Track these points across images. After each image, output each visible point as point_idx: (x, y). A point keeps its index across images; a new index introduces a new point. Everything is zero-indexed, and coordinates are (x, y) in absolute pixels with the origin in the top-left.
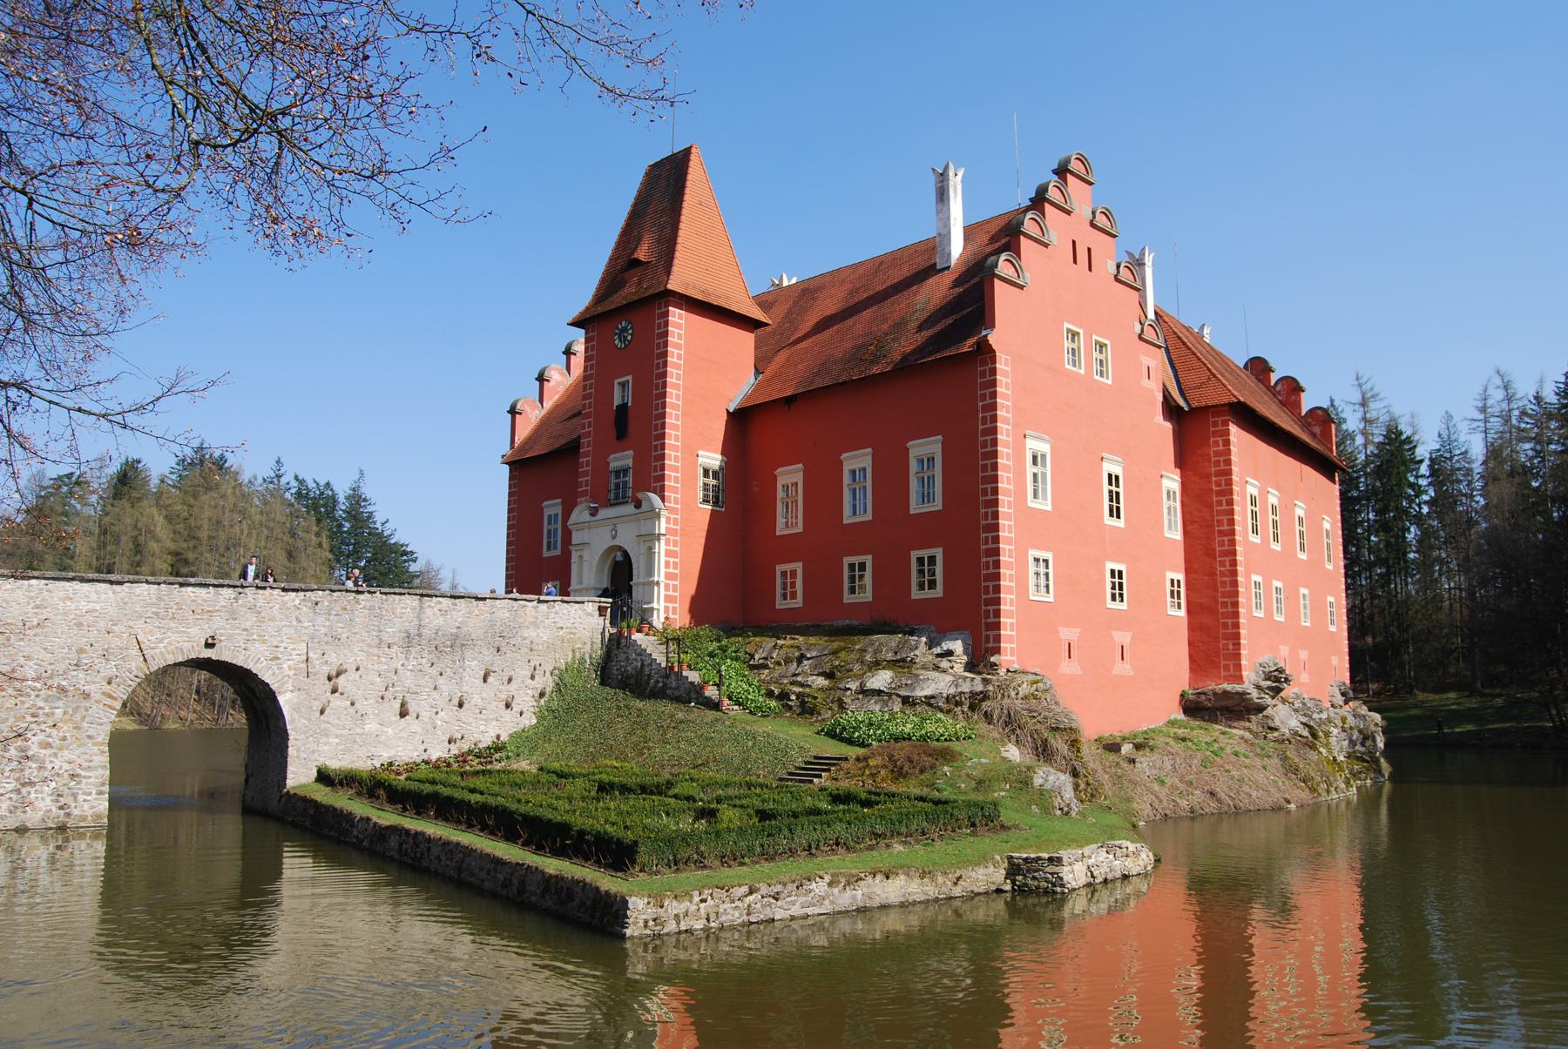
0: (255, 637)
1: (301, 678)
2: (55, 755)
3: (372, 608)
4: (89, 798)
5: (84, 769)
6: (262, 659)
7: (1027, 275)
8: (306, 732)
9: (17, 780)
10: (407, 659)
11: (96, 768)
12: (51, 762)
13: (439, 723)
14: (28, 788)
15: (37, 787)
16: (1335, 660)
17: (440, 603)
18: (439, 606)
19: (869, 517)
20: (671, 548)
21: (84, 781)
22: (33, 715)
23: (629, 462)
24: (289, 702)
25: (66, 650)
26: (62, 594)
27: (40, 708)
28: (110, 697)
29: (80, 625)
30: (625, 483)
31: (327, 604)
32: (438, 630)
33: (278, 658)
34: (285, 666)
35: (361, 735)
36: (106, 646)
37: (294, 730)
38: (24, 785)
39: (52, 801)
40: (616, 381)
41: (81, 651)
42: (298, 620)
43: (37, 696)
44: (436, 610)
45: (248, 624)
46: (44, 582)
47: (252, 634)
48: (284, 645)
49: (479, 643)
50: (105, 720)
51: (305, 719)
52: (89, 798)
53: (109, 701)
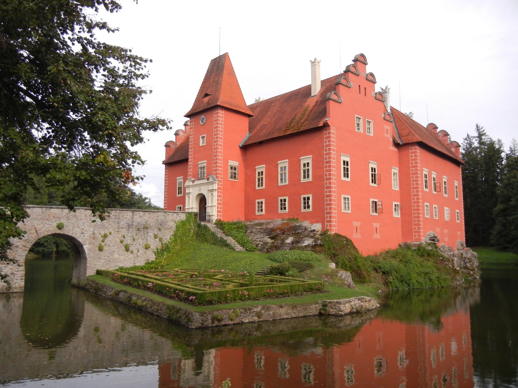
2: (6, 267)
3: (116, 216)
4: (18, 281)
5: (16, 271)
7: (342, 98)
8: (93, 258)
11: (20, 271)
12: (5, 269)
13: (139, 255)
16: (459, 233)
17: (139, 214)
19: (287, 183)
20: (219, 194)
21: (16, 275)
23: (205, 165)
24: (87, 248)
28: (25, 247)
30: (204, 172)
33: (83, 233)
34: (86, 235)
35: (112, 259)
37: (89, 257)
40: (201, 136)
44: (138, 216)
48: (86, 228)
50: (24, 254)
52: (18, 281)
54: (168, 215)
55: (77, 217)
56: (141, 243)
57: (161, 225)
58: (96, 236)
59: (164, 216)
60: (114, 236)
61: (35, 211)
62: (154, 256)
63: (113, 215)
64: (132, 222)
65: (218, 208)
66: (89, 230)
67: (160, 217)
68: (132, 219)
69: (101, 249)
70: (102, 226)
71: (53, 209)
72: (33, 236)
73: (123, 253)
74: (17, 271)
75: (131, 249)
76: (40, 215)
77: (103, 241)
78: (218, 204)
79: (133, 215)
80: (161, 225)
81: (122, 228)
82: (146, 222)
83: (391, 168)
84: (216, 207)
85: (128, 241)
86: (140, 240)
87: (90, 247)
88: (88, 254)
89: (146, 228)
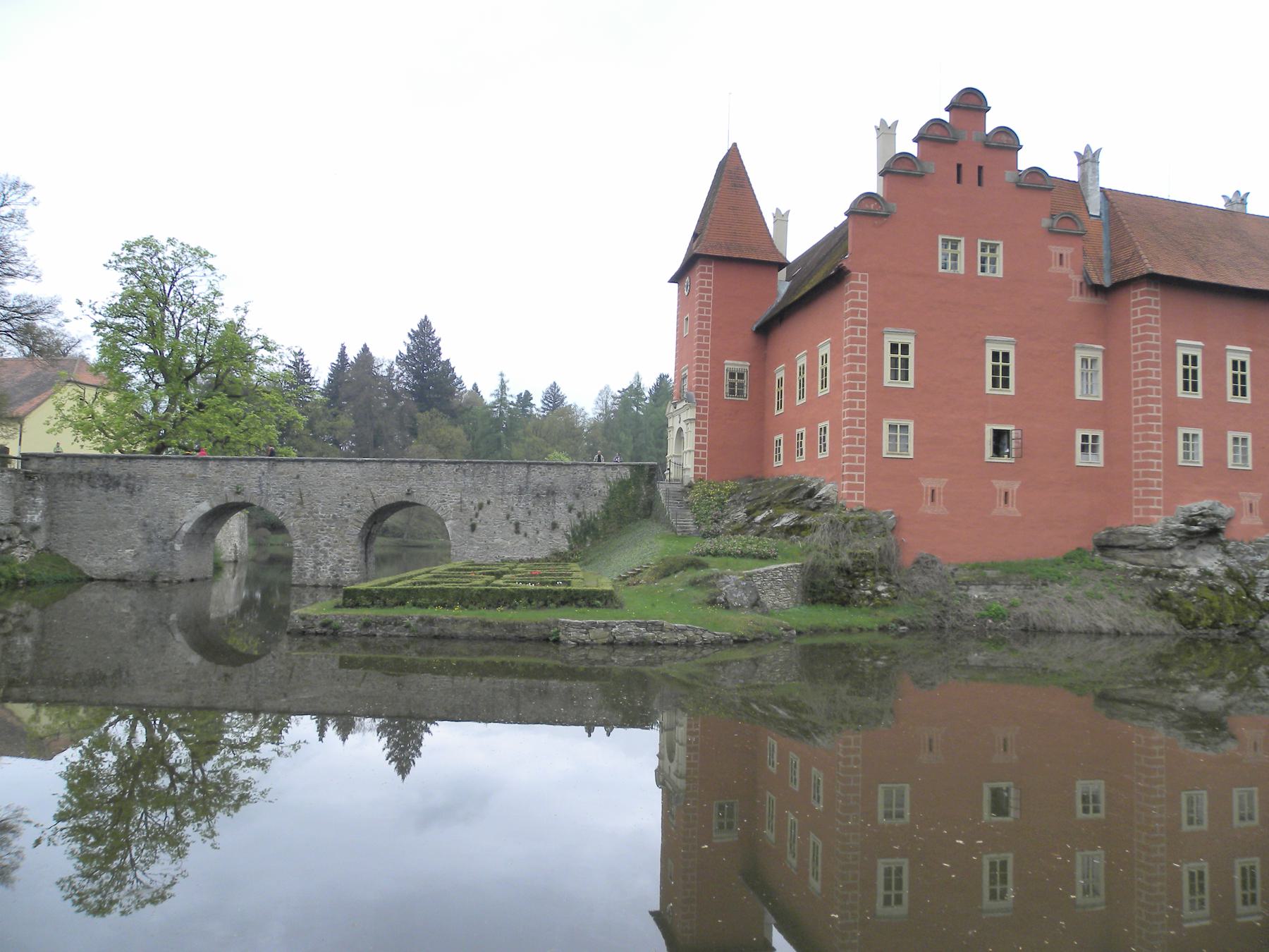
3: (498, 472)
9: (314, 561)
22: (322, 530)
24: (451, 525)
26: (334, 469)
29: (343, 484)
38: (318, 564)
41: (343, 498)
54: (596, 469)
57: (581, 489)
58: (465, 506)
59: (586, 472)
61: (371, 466)
62: (567, 543)
65: (696, 454)
68: (527, 477)
69: (473, 528)
71: (397, 465)
72: (369, 505)
74: (347, 558)
75: (523, 529)
76: (378, 473)
77: (477, 515)
78: (697, 447)
80: (581, 489)
81: (509, 493)
83: (1074, 349)
84: (693, 453)
85: (520, 515)
89: (551, 492)
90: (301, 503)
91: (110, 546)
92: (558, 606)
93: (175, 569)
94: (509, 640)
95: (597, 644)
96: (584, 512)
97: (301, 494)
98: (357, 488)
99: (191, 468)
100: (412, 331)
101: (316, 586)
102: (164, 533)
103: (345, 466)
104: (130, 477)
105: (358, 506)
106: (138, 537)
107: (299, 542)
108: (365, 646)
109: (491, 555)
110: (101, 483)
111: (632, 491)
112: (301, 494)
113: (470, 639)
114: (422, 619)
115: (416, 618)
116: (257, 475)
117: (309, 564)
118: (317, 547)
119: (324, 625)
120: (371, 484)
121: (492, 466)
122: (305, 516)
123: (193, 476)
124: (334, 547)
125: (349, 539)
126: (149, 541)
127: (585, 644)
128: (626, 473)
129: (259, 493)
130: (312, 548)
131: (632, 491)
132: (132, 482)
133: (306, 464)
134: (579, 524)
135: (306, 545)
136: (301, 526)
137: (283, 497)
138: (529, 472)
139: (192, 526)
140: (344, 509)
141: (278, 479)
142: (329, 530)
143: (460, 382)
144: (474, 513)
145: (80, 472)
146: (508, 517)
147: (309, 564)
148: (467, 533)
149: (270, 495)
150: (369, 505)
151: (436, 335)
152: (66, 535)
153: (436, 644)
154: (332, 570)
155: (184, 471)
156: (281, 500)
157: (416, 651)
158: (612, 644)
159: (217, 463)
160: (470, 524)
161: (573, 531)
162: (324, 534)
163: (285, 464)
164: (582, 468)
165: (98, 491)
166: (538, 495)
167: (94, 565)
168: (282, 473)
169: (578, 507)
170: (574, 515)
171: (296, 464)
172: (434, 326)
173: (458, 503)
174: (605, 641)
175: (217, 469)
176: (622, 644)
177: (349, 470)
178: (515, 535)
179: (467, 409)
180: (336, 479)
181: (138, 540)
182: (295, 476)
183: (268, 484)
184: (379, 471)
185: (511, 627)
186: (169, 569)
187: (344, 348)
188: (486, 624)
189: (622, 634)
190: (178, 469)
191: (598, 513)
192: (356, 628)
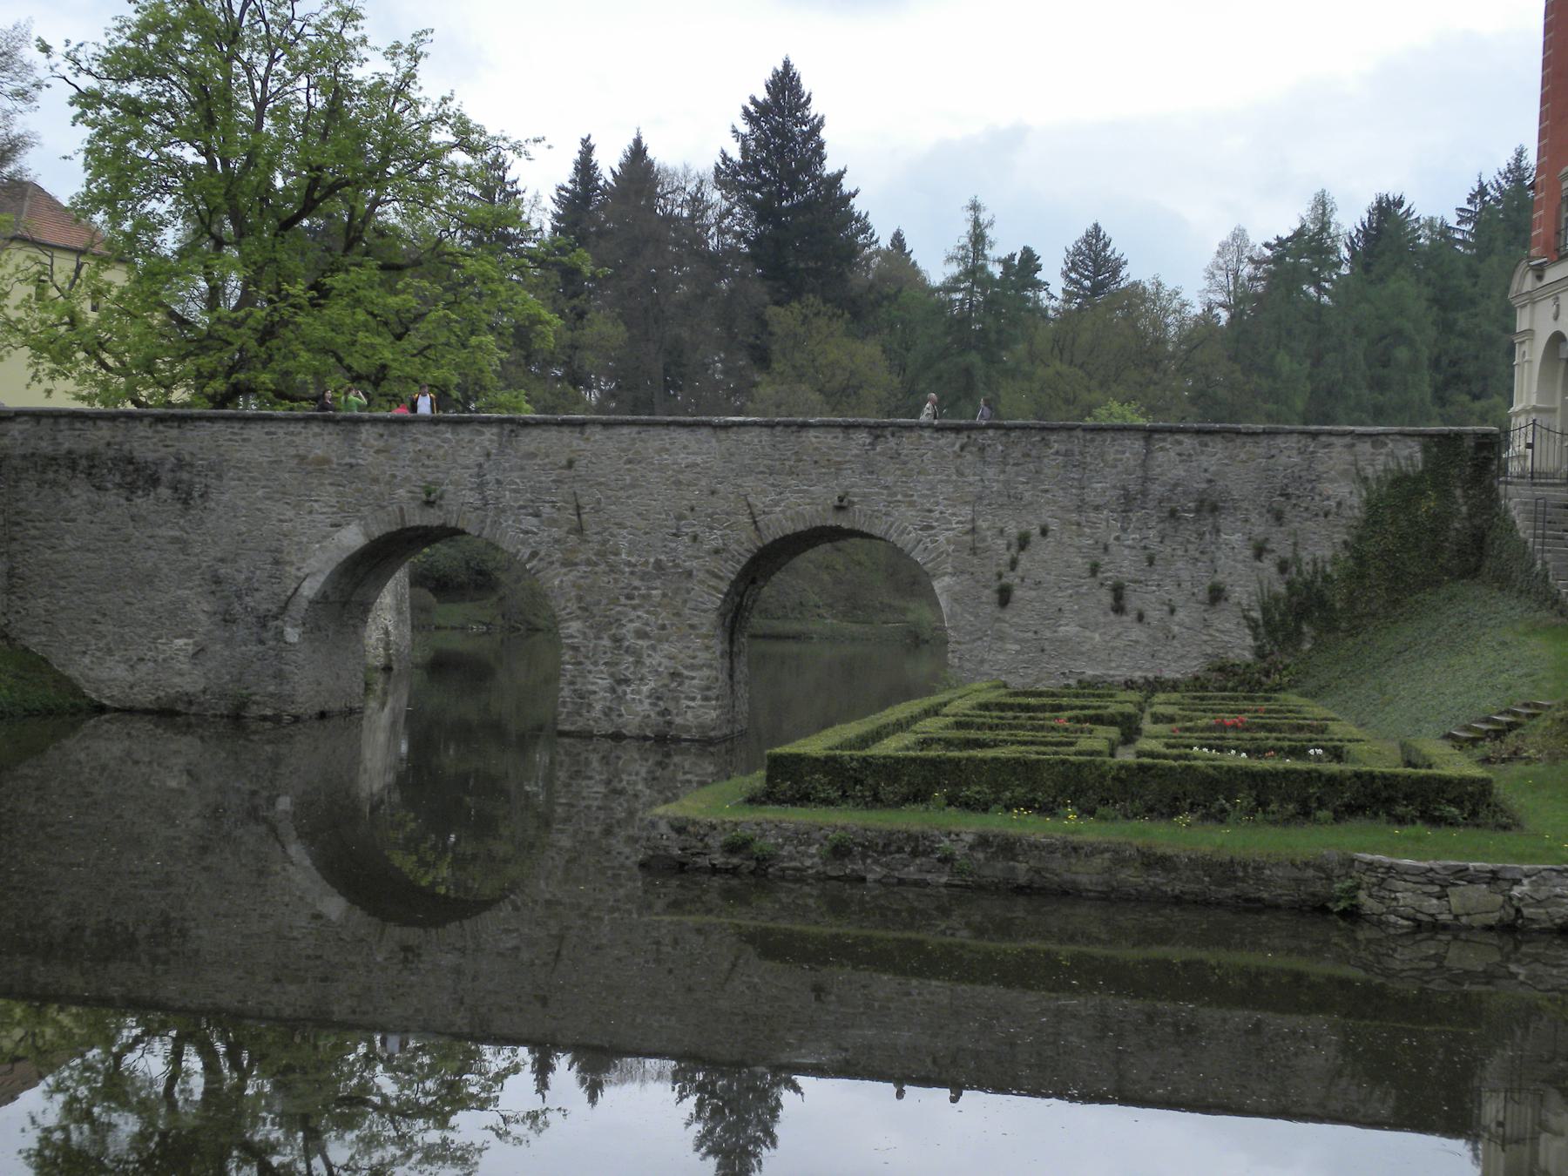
0: (899, 497)
1: (965, 555)
2: (653, 648)
3: (1068, 453)
4: (692, 704)
5: (686, 667)
6: (910, 528)
8: (971, 633)
9: (612, 675)
10: (1124, 530)
11: (701, 667)
12: (649, 656)
13: (1176, 629)
14: (624, 687)
15: (633, 687)
17: (1180, 443)
18: (1178, 448)
22: (629, 597)
24: (948, 589)
25: (664, 516)
26: (657, 444)
27: (636, 588)
29: (678, 483)
31: (1000, 448)
32: (1176, 485)
33: (932, 528)
34: (941, 538)
36: (710, 511)
37: (954, 628)
38: (619, 682)
39: (651, 704)
41: (680, 517)
42: (960, 473)
43: (632, 573)
44: (1172, 454)
45: (890, 479)
46: (635, 429)
47: (895, 494)
48: (941, 508)
49: (1245, 505)
50: (709, 606)
51: (971, 613)
52: (692, 704)
53: (713, 582)
54: (1329, 445)
55: (905, 463)
56: (1185, 575)
57: (1288, 496)
58: (984, 540)
60: (1060, 543)
61: (747, 438)
62: (1250, 641)
63: (1057, 453)
64: (1146, 479)
66: (954, 514)
67: (1283, 459)
68: (1144, 465)
69: (1004, 596)
70: (1005, 500)
71: (812, 433)
73: (1102, 619)
74: (692, 667)
75: (1133, 601)
77: (1013, 564)
79: (1149, 452)
80: (1288, 496)
81: (1097, 508)
82: (1210, 481)
85: (1125, 564)
86: (1179, 564)
87: (958, 588)
88: (953, 616)
89: (1210, 507)
90: (579, 530)
91: (141, 631)
92: (1338, 818)
93: (287, 688)
94: (1219, 904)
95: (1470, 928)
96: (1297, 560)
97: (578, 508)
98: (713, 493)
99: (320, 442)
100: (754, 101)
101: (617, 737)
102: (261, 601)
103: (683, 436)
104: (180, 464)
105: (713, 540)
106: (201, 608)
107: (575, 626)
108: (837, 906)
109: (1052, 667)
110: (117, 479)
111: (1429, 504)
112: (578, 508)
113: (1112, 897)
114: (983, 841)
115: (969, 838)
116: (471, 460)
117: (599, 682)
118: (617, 640)
119: (732, 848)
120: (749, 483)
121: (1053, 437)
122: (588, 562)
123: (327, 461)
124: (660, 641)
125: (695, 621)
126: (228, 620)
127: (1436, 927)
128: (1410, 455)
129: (479, 503)
130: (606, 642)
131: (1429, 504)
132: (185, 476)
133: (588, 430)
134: (1281, 589)
135: (591, 633)
136: (580, 587)
137: (537, 515)
138: (1149, 452)
139: (325, 583)
140: (682, 546)
141: (522, 469)
142: (646, 597)
143: (866, 228)
144: (1007, 557)
145: (70, 452)
146: (1094, 570)
147: (599, 682)
148: (990, 609)
149: (504, 511)
150: (744, 536)
151: (814, 109)
152: (41, 602)
153: (1020, 909)
154: (656, 697)
155: (302, 451)
156: (530, 522)
157: (968, 924)
158: (1512, 929)
159: (380, 429)
160: (996, 585)
161: (1265, 610)
162: (634, 608)
163: (535, 432)
164: (1293, 441)
165: (111, 498)
166: (1173, 513)
167: (105, 675)
168: (533, 456)
169: (1281, 546)
170: (1268, 566)
171: (566, 430)
172: (806, 87)
173: (967, 533)
174: (1492, 919)
175: (380, 444)
176: (1542, 931)
177: (694, 447)
178: (1112, 616)
179: (887, 297)
180: (662, 468)
181: (202, 617)
182: (564, 462)
183: (498, 482)
184: (768, 450)
185: (1226, 870)
186: (271, 688)
187: (587, 149)
188: (1153, 861)
189: (1539, 903)
190: (290, 444)
191: (1334, 561)
192: (812, 858)
